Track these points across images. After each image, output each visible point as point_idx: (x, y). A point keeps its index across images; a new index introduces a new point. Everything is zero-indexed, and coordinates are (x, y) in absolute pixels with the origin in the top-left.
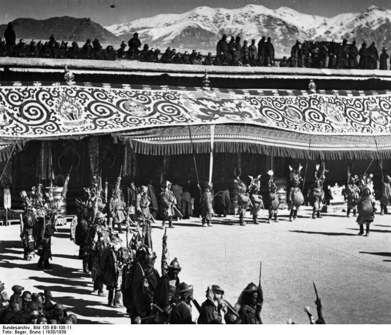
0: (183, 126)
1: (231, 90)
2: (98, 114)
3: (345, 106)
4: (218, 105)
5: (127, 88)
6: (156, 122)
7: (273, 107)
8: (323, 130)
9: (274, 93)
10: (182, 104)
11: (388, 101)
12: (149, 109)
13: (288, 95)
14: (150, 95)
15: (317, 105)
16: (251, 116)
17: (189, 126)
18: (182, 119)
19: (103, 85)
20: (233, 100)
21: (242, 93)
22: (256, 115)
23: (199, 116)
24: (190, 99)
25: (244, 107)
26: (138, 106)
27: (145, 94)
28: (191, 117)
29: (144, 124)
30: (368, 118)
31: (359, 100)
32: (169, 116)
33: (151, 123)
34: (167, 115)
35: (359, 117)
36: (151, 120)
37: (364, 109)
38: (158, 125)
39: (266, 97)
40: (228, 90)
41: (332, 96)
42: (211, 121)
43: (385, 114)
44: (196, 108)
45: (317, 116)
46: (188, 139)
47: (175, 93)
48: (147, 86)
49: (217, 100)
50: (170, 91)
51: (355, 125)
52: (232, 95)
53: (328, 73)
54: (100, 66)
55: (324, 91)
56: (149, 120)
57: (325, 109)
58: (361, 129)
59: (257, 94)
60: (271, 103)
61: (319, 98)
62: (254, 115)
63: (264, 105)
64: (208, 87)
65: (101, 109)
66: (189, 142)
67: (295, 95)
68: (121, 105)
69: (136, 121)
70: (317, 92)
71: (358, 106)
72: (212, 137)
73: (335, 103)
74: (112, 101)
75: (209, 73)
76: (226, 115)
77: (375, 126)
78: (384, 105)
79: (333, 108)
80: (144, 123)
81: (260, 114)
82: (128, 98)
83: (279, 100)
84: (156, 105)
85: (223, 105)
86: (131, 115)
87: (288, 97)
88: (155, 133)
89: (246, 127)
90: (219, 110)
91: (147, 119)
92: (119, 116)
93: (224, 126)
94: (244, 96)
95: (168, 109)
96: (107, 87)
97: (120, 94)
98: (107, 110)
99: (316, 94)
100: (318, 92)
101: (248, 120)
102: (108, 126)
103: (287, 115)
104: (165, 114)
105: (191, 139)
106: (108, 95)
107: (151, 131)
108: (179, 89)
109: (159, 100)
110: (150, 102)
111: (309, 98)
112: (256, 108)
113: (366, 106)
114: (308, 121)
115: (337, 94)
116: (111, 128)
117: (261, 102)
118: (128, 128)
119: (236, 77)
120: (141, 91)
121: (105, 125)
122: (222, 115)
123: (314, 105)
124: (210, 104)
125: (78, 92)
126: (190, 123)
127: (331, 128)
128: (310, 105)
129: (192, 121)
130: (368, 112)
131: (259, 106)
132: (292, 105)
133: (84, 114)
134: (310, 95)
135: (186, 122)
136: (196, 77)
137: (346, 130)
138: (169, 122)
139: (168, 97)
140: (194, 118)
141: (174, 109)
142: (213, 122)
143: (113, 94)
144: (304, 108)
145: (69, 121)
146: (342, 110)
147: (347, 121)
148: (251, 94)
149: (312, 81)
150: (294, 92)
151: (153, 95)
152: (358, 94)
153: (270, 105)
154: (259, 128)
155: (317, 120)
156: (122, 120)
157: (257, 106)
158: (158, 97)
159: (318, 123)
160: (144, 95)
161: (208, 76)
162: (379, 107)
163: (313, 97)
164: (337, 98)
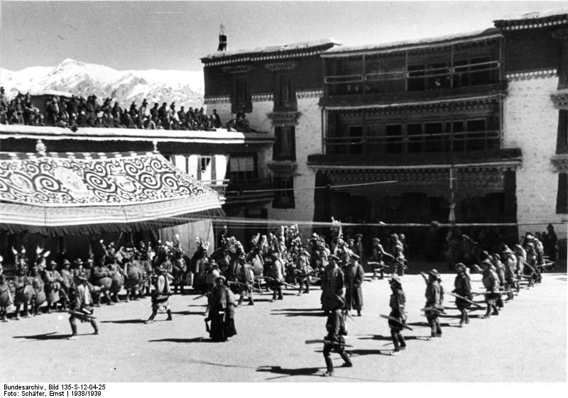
11: (134, 164)
13: (10, 159)
15: (48, 170)
30: (113, 185)
31: (100, 163)
35: (101, 183)
37: (107, 174)
41: (66, 159)
43: (133, 179)
51: (99, 193)
53: (59, 132)
55: (56, 153)
57: (60, 175)
58: (106, 198)
61: (52, 162)
71: (100, 170)
73: (71, 168)
77: (122, 194)
78: (130, 168)
79: (70, 174)
99: (46, 158)
103: (12, 184)
115: (73, 157)
123: (45, 170)
127: (70, 198)
128: (40, 170)
130: (112, 177)
132: (17, 171)
134: (40, 159)
137: (88, 200)
144: (33, 175)
146: (81, 176)
147: (89, 189)
149: (40, 141)
152: (98, 157)
162: (124, 171)
163: (43, 161)
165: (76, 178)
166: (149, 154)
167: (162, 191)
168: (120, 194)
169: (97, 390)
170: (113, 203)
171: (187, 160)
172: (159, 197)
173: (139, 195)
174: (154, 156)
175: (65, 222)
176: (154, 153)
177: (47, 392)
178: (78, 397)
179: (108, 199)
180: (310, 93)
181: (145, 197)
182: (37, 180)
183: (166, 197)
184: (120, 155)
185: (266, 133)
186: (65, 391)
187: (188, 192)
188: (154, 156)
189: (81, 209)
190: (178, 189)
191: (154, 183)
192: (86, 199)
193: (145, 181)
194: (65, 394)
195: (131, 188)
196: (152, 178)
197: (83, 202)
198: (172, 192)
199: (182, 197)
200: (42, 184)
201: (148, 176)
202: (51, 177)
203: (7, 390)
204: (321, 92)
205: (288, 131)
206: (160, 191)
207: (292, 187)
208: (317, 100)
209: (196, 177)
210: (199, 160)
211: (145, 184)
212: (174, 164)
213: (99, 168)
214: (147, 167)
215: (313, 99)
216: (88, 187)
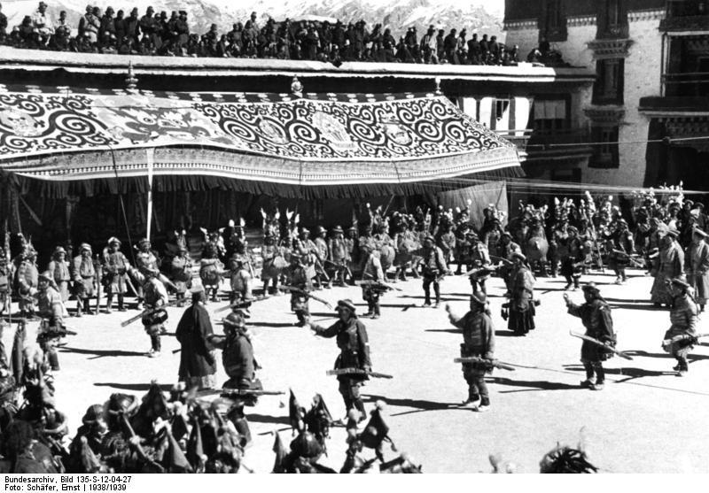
0: (102, 152)
1: (172, 93)
3: (348, 118)
4: (155, 117)
6: (57, 145)
8: (319, 154)
9: (239, 98)
11: (410, 109)
12: (42, 123)
13: (260, 101)
14: (42, 101)
15: (305, 116)
16: (208, 134)
17: (112, 150)
18: (99, 140)
23: (126, 135)
24: (108, 108)
25: (196, 120)
26: (23, 119)
27: (33, 99)
28: (114, 136)
30: (383, 135)
31: (367, 108)
33: (48, 147)
34: (73, 133)
36: (48, 142)
37: (375, 122)
38: (59, 150)
39: (228, 104)
40: (167, 93)
41: (327, 102)
42: (146, 142)
44: (121, 122)
45: (307, 133)
47: (83, 98)
48: (34, 87)
49: (152, 109)
50: (74, 95)
51: (365, 146)
52: (173, 100)
53: (318, 67)
56: (45, 141)
58: (374, 152)
59: (214, 99)
60: (235, 113)
61: (309, 105)
62: (211, 132)
63: (225, 116)
64: (135, 88)
66: (113, 175)
67: (271, 101)
69: (22, 144)
70: (304, 97)
71: (367, 116)
72: (150, 167)
73: (332, 113)
76: (169, 132)
77: (393, 147)
78: (405, 114)
80: (36, 146)
81: (222, 131)
83: (247, 109)
84: (53, 117)
86: (12, 134)
88: (55, 162)
89: (202, 150)
90: (156, 125)
91: (40, 140)
93: (168, 150)
94: (194, 103)
95: (74, 124)
99: (302, 100)
100: (305, 96)
101: (203, 140)
103: (261, 132)
104: (69, 132)
107: (50, 159)
108: (88, 92)
109: (57, 110)
110: (42, 112)
112: (214, 122)
113: (377, 116)
114: (295, 140)
115: (335, 99)
117: (220, 112)
118: (9, 155)
119: (177, 73)
120: (25, 95)
122: (162, 132)
123: (301, 115)
126: (114, 147)
127: (330, 151)
128: (295, 116)
129: (116, 143)
130: (382, 126)
131: (218, 118)
132: (268, 116)
134: (294, 101)
135: (105, 144)
136: (111, 74)
137: (352, 154)
138: (79, 145)
140: (118, 137)
141: (84, 123)
142: (150, 143)
144: (286, 121)
146: (344, 123)
147: (352, 140)
148: (203, 100)
149: (296, 79)
151: (46, 101)
152: (366, 100)
154: (222, 153)
157: (214, 119)
158: (55, 104)
159: (309, 144)
160: (31, 101)
161: (133, 72)
162: (397, 118)
163: (298, 104)
164: (334, 105)
165: (338, 126)
166: (430, 96)
167: (445, 144)
168: (390, 146)
169: (121, 483)
170: (382, 159)
171: (478, 104)
172: (441, 151)
173: (415, 148)
174: (436, 99)
177: (59, 486)
178: (97, 491)
179: (376, 153)
180: (647, 14)
181: (423, 151)
182: (292, 128)
183: (449, 151)
184: (393, 98)
185: (585, 67)
186: (82, 485)
187: (479, 145)
188: (436, 99)
189: (343, 164)
190: (465, 142)
191: (434, 133)
192: (349, 153)
193: (423, 131)
194: (82, 488)
196: (433, 128)
197: (346, 156)
198: (458, 144)
199: (471, 151)
201: (427, 124)
203: (9, 483)
204: (662, 12)
205: (615, 65)
206: (442, 143)
207: (617, 140)
208: (657, 23)
209: (488, 126)
210: (493, 104)
211: (423, 135)
212: (462, 108)
213: (366, 114)
214: (426, 112)
215: (651, 21)
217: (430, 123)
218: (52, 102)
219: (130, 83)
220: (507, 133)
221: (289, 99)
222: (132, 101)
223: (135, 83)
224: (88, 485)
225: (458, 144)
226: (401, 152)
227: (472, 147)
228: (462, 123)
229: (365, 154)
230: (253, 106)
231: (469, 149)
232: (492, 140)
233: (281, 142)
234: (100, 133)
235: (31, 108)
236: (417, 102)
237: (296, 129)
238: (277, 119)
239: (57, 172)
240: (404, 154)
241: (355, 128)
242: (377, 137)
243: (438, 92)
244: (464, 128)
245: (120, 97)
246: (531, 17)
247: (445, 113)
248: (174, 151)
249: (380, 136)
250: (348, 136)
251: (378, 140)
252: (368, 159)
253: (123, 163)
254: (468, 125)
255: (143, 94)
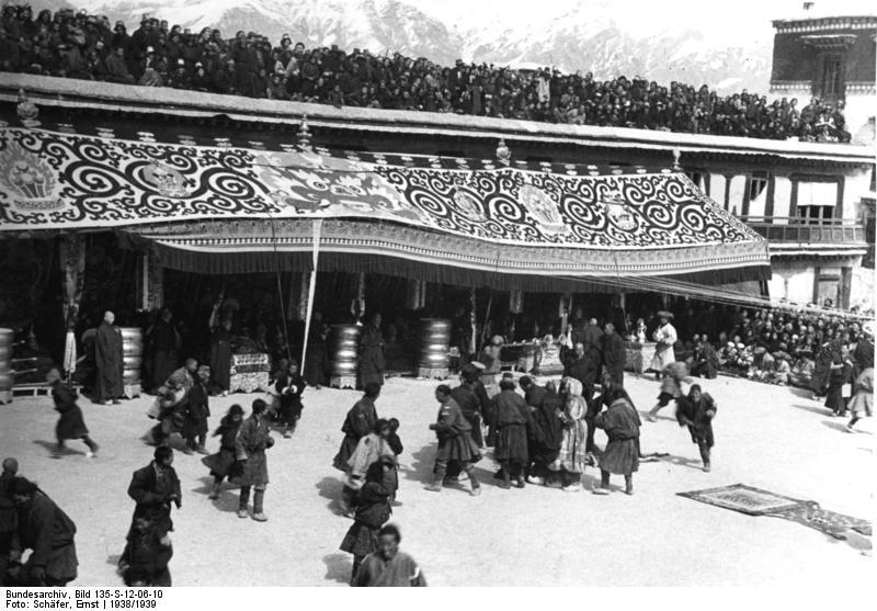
0: (262, 220)
1: (352, 153)
2: (88, 188)
4: (328, 181)
5: (147, 139)
6: (207, 209)
7: (430, 189)
9: (432, 163)
10: (256, 176)
11: (640, 187)
12: (192, 182)
13: (457, 168)
14: (195, 155)
15: (511, 190)
16: (390, 205)
17: (271, 219)
18: (258, 206)
19: (99, 131)
20: (356, 172)
21: (374, 160)
22: (400, 203)
23: (290, 201)
24: (272, 167)
25: (377, 187)
26: (172, 176)
27: (185, 152)
28: (276, 202)
29: (184, 213)
30: (603, 217)
31: (587, 182)
32: (231, 197)
33: (197, 211)
34: (227, 196)
36: (197, 205)
37: (595, 200)
38: (210, 215)
39: (418, 169)
40: (347, 152)
41: (539, 173)
42: (313, 211)
43: (634, 211)
44: (285, 185)
45: (510, 210)
46: (269, 245)
48: (187, 137)
49: (325, 171)
50: (233, 150)
52: (353, 163)
54: (92, 92)
56: (193, 204)
58: (589, 237)
59: (401, 163)
60: (426, 181)
61: (516, 176)
62: (395, 203)
63: (413, 184)
64: (307, 145)
65: (94, 179)
66: (272, 249)
68: (135, 173)
69: (166, 206)
70: (511, 165)
71: (586, 193)
72: (316, 242)
74: (117, 164)
75: (310, 118)
77: (614, 233)
78: (632, 193)
80: (182, 210)
82: (149, 159)
83: (441, 177)
85: (337, 181)
86: (156, 193)
87: (457, 172)
88: (203, 230)
90: (329, 191)
91: (188, 203)
92: (132, 193)
93: (339, 223)
94: (377, 166)
95: (231, 185)
96: (106, 137)
97: (134, 151)
98: (106, 181)
99: (509, 169)
100: (513, 165)
101: (383, 214)
102: (107, 214)
103: (455, 205)
104: (223, 195)
105: (275, 246)
106: (109, 151)
108: (250, 147)
109: (212, 166)
110: (194, 169)
111: (497, 175)
112: (399, 190)
113: (599, 193)
116: (116, 218)
117: (407, 178)
118: (150, 219)
119: (361, 127)
120: (176, 147)
121: (102, 212)
122: (335, 200)
123: (505, 188)
124: (312, 179)
125: (46, 142)
126: (275, 215)
127: (536, 234)
130: (603, 205)
131: (404, 187)
132: (465, 186)
133: (59, 187)
134: (499, 170)
136: (282, 124)
137: (563, 239)
138: (233, 211)
139: (229, 160)
141: (241, 184)
142: (319, 213)
143: (119, 150)
144: (487, 194)
145: (27, 199)
146: (556, 201)
147: (565, 222)
150: (469, 163)
152: (587, 172)
153: (425, 184)
154: (404, 229)
155: (511, 217)
156: (138, 202)
157: (400, 187)
158: (210, 160)
159: (511, 223)
162: (622, 197)
164: (547, 177)
165: (549, 204)
166: (666, 172)
167: (677, 233)
168: (610, 232)
170: (599, 246)
172: (672, 241)
173: (641, 236)
174: (673, 176)
175: (517, 268)
176: (674, 171)
177: (73, 602)
178: (120, 609)
179: (593, 239)
181: (650, 239)
182: (492, 203)
183: (682, 242)
184: (620, 171)
186: (101, 601)
187: (720, 236)
188: (673, 176)
190: (704, 231)
191: (666, 219)
193: (652, 215)
194: (101, 605)
195: (628, 224)
196: (665, 212)
197: (556, 241)
198: (694, 234)
199: (708, 243)
200: (499, 211)
201: (659, 207)
202: (512, 200)
203: (11, 598)
206: (674, 232)
209: (739, 212)
210: (747, 183)
211: (652, 219)
213: (585, 189)
214: (659, 192)
216: (564, 218)
217: (664, 206)
218: (207, 157)
219: (302, 138)
220: (762, 220)
221: (493, 167)
222: (304, 160)
223: (307, 138)
224: (108, 601)
225: (694, 234)
226: (623, 239)
227: (712, 238)
228: (702, 208)
229: (578, 239)
230: (448, 173)
231: (707, 240)
232: (739, 231)
233: (478, 219)
234: (260, 197)
235: (181, 163)
236: (649, 178)
237: (497, 205)
238: (475, 191)
239: (199, 242)
240: (626, 242)
241: (570, 207)
242: (596, 220)
243: (676, 167)
244: (704, 214)
245: (289, 154)
246: (803, 79)
247: (683, 193)
248: (347, 225)
249: (599, 218)
250: (560, 217)
251: (597, 223)
252: (581, 245)
253: (284, 235)
254: (710, 210)
255: (316, 152)
